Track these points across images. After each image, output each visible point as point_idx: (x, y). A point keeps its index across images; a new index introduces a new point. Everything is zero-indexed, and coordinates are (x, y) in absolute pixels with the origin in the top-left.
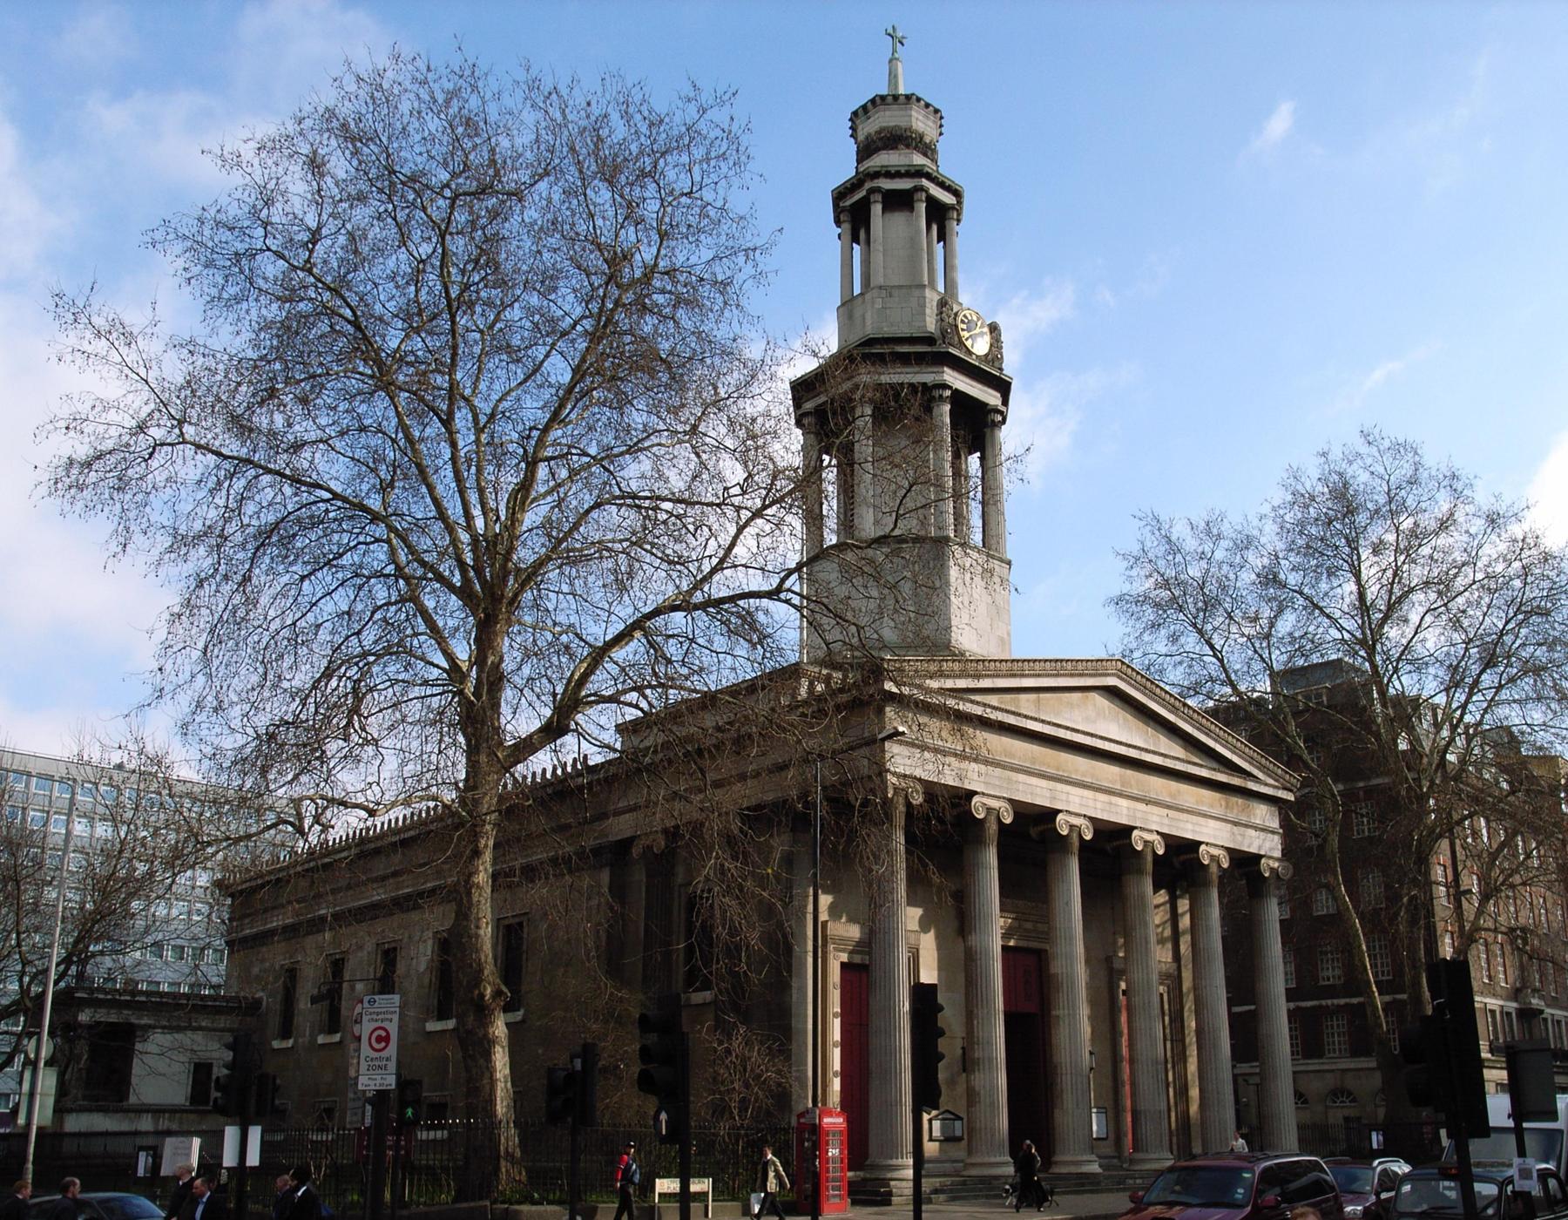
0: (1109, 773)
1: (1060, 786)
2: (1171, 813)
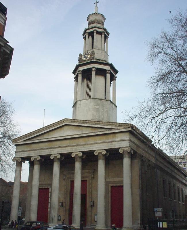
0: (68, 142)
1: (51, 150)
2: (84, 146)
